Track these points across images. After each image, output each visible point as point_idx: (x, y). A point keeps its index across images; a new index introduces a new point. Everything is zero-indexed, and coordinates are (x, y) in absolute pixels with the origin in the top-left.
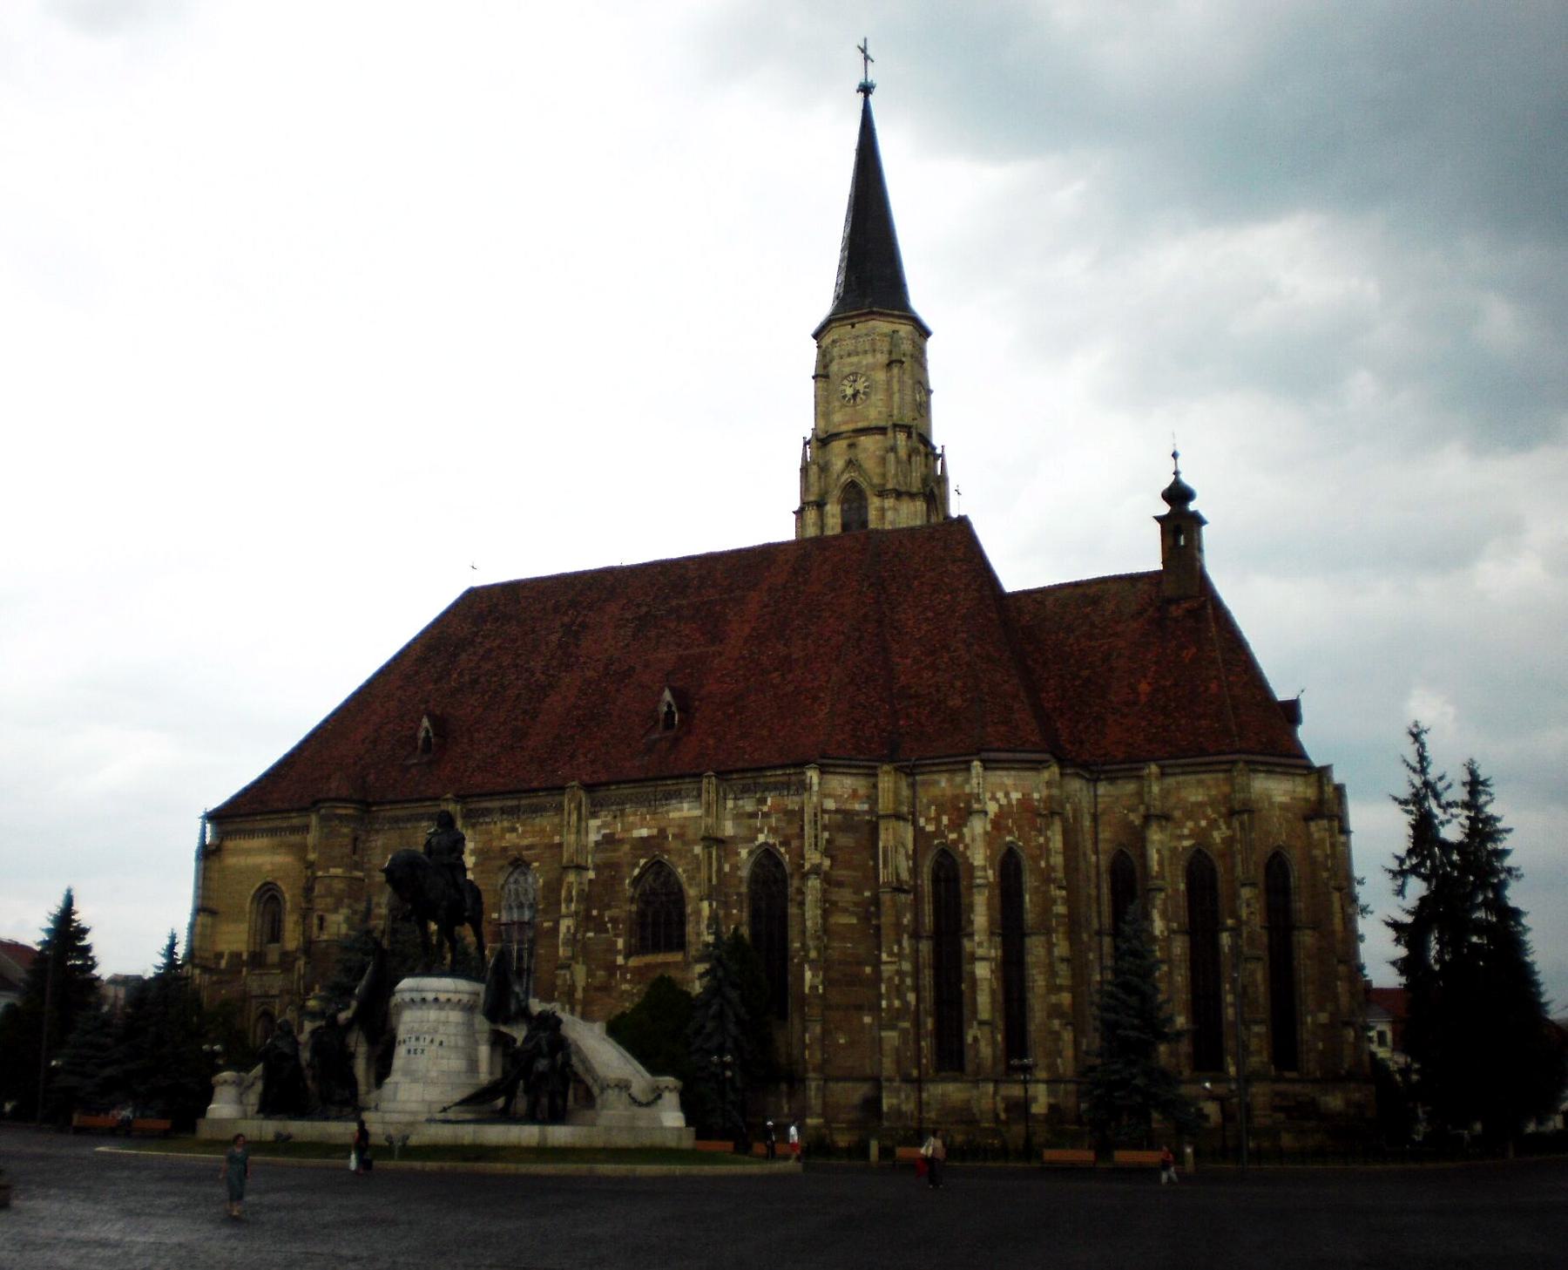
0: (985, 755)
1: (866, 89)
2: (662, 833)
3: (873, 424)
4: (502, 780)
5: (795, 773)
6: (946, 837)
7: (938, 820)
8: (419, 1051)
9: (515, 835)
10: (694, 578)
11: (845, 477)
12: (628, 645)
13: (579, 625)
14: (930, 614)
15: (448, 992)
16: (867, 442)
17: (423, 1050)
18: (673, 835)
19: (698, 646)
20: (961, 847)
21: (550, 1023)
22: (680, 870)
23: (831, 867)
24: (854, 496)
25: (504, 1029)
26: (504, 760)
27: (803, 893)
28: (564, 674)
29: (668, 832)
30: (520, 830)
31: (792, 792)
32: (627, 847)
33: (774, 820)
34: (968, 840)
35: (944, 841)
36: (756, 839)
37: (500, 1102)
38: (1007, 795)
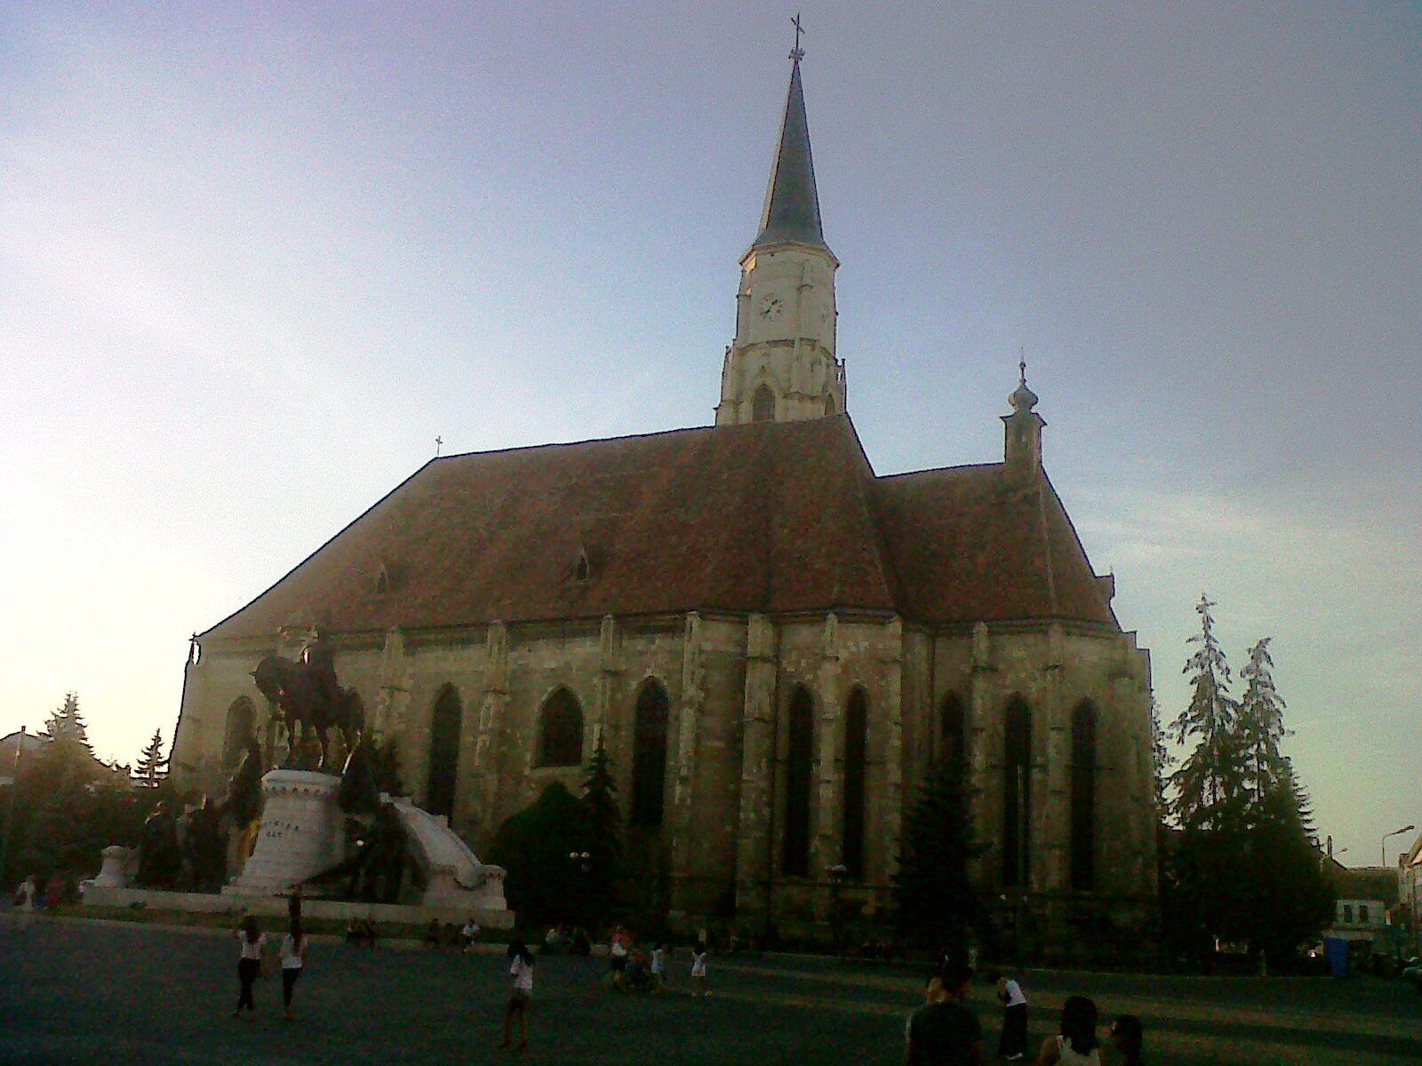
0: (837, 610)
1: (797, 56)
2: (568, 664)
11: (758, 382)
15: (305, 783)
16: (780, 352)
21: (388, 814)
22: (580, 697)
23: (705, 698)
24: (764, 397)
25: (357, 818)
35: (801, 681)
37: (348, 880)
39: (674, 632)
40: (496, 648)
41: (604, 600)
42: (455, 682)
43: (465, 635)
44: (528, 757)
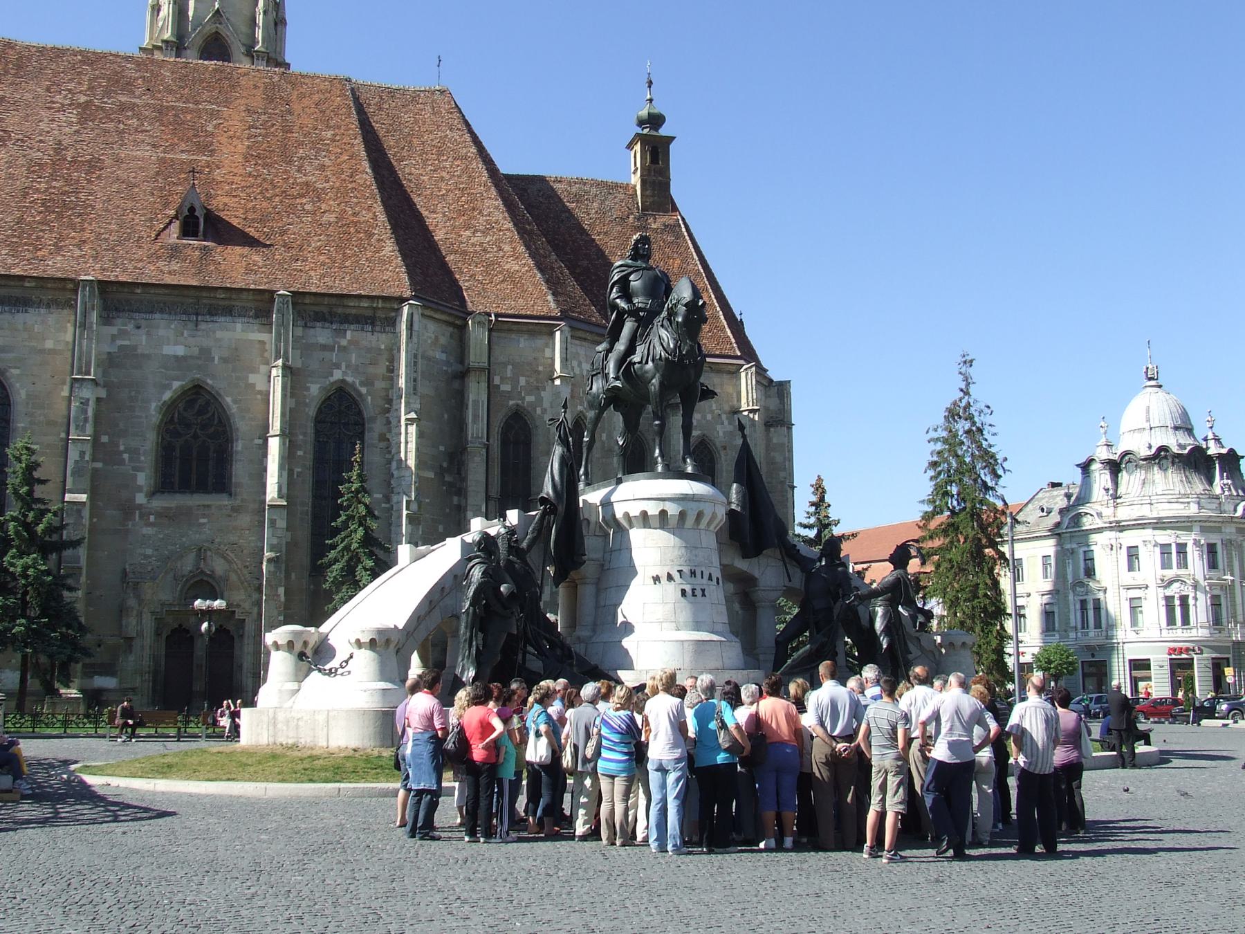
5: (383, 308)
7: (515, 381)
8: (699, 593)
10: (137, 79)
11: (211, 29)
14: (444, 174)
17: (703, 591)
18: (220, 358)
19: (182, 151)
20: (539, 411)
22: (229, 400)
27: (388, 440)
29: (213, 354)
31: (378, 328)
33: (354, 355)
34: (546, 404)
35: (520, 402)
36: (332, 376)
38: (580, 365)
39: (373, 324)
41: (248, 271)
43: (17, 292)
44: (142, 479)
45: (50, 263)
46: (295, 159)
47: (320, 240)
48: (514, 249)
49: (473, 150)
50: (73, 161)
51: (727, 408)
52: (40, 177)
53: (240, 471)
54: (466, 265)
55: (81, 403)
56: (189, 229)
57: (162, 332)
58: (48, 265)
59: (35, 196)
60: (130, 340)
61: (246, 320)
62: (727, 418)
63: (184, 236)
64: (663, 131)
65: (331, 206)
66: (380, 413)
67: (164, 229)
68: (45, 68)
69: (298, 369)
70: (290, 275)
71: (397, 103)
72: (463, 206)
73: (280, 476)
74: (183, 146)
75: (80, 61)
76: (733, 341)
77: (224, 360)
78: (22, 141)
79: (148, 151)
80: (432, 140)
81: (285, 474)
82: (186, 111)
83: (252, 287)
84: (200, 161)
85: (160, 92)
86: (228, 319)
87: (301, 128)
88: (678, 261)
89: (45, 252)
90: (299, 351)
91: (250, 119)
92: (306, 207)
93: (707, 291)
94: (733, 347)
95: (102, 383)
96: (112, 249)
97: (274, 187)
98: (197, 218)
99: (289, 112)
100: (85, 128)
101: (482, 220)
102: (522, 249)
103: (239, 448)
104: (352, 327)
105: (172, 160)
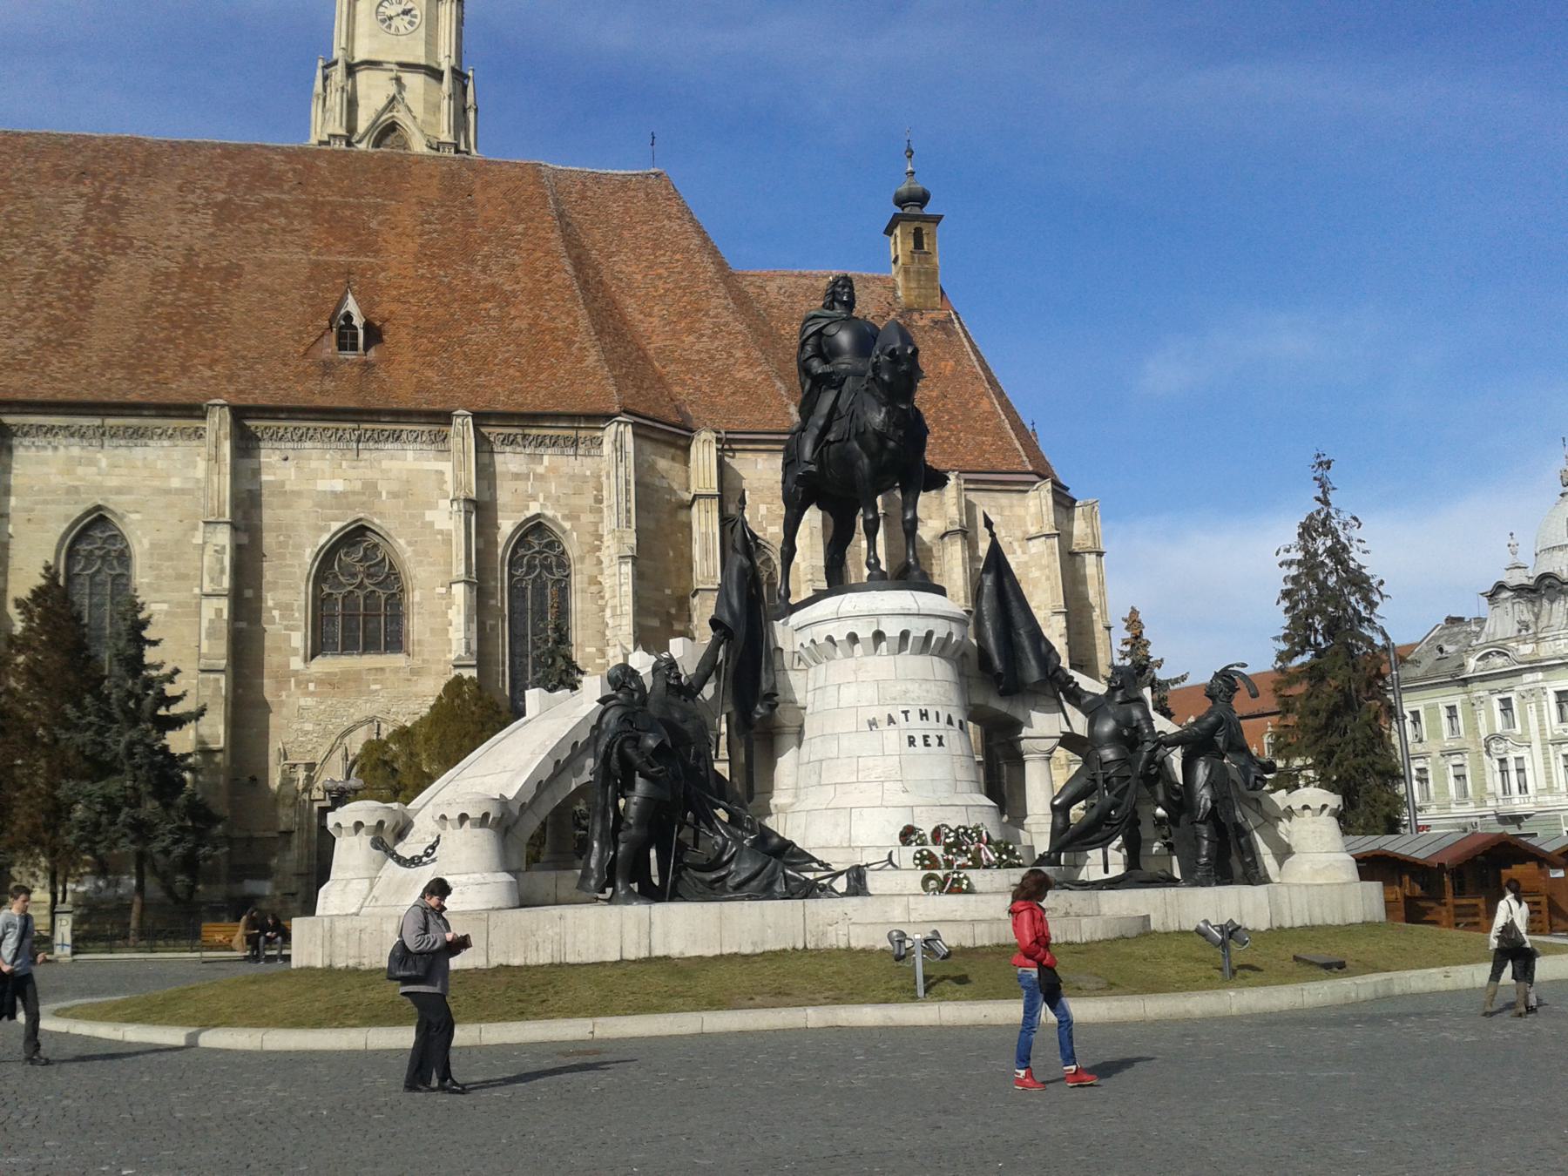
2: (371, 488)
3: (423, 61)
4: (62, 386)
6: (765, 529)
9: (94, 469)
12: (212, 235)
13: (116, 198)
14: (661, 271)
16: (415, 81)
18: (388, 493)
22: (402, 542)
26: (54, 361)
28: (113, 257)
30: (104, 463)
31: (580, 452)
32: (306, 504)
33: (553, 484)
36: (527, 508)
40: (226, 447)
41: (421, 387)
42: (115, 503)
44: (298, 640)
45: (174, 386)
46: (479, 257)
47: (508, 351)
48: (748, 354)
49: (697, 241)
50: (207, 268)
51: (1019, 534)
52: (166, 288)
53: (417, 626)
54: (690, 376)
55: (216, 551)
56: (346, 338)
57: (314, 464)
58: (171, 389)
59: (159, 310)
60: (275, 474)
61: (418, 446)
62: (1020, 546)
63: (340, 350)
64: (928, 210)
65: (523, 311)
66: (588, 552)
67: (315, 342)
68: (177, 165)
69: (486, 502)
70: (472, 392)
71: (604, 190)
72: (685, 307)
73: (468, 629)
74: (340, 246)
75: (220, 155)
76: (1023, 453)
77: (394, 495)
78: (146, 248)
79: (297, 253)
80: (647, 232)
81: (474, 627)
82: (346, 205)
83: (425, 407)
84: (361, 263)
85: (313, 186)
86: (397, 445)
87: (486, 222)
88: (951, 363)
89: (168, 373)
90: (486, 482)
91: (422, 214)
92: (492, 313)
93: (989, 397)
94: (1023, 461)
95: (243, 527)
96: (251, 368)
97: (452, 290)
98: (355, 328)
99: (471, 203)
100: (222, 230)
101: (708, 322)
102: (756, 354)
103: (417, 599)
104: (550, 451)
105: (326, 263)
